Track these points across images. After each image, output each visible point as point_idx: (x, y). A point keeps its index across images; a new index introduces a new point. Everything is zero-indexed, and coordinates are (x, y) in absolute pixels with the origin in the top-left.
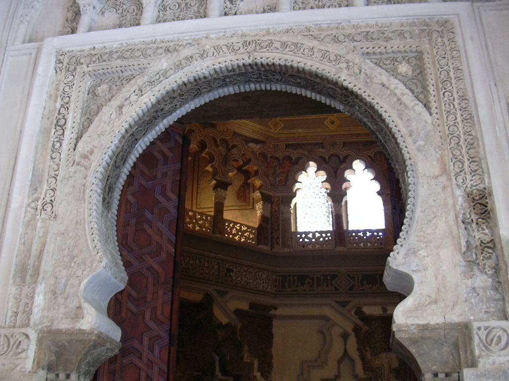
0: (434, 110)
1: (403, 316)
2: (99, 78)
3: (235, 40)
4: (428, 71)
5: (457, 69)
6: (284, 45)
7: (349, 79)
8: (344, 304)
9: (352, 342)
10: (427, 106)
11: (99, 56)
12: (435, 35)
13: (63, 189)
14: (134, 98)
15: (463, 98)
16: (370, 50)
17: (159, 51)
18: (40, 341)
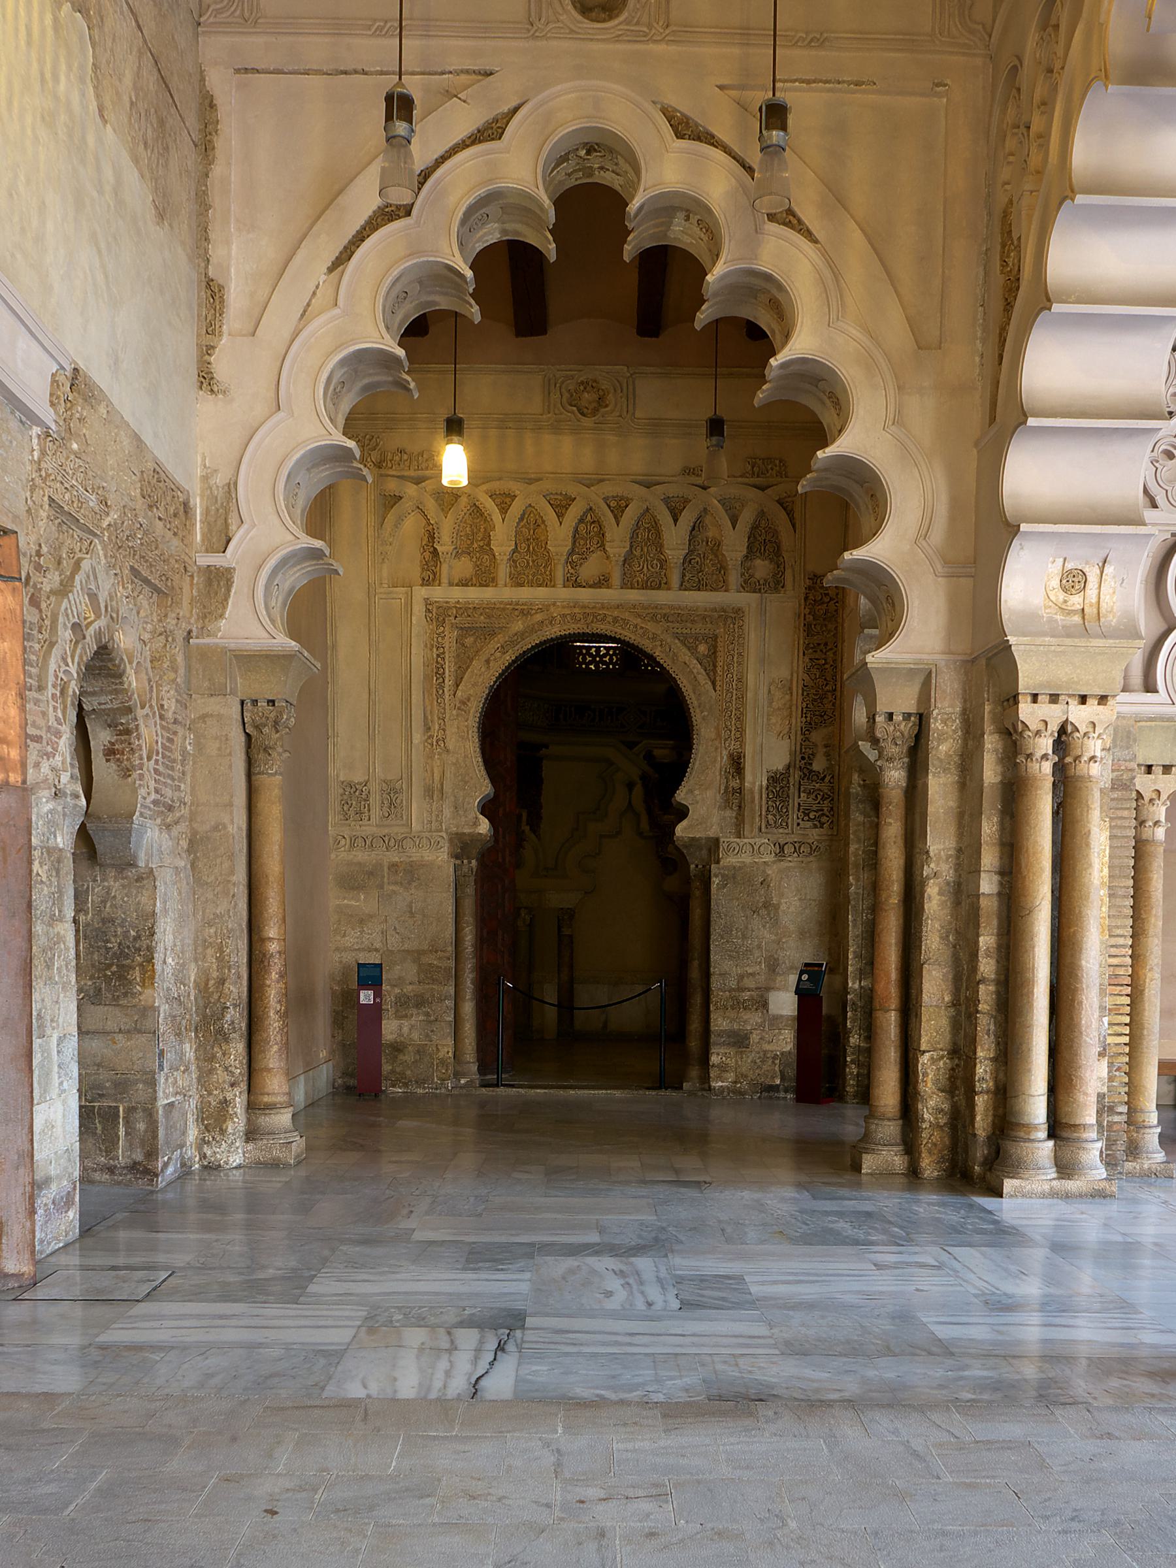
0: (718, 688)
1: (681, 830)
2: (465, 631)
3: (577, 610)
4: (719, 654)
5: (740, 654)
6: (616, 620)
7: (662, 655)
8: (631, 746)
9: (638, 790)
10: (714, 683)
11: (464, 609)
12: (729, 621)
13: (451, 730)
14: (498, 654)
15: (739, 680)
16: (679, 631)
17: (516, 613)
18: (451, 841)
